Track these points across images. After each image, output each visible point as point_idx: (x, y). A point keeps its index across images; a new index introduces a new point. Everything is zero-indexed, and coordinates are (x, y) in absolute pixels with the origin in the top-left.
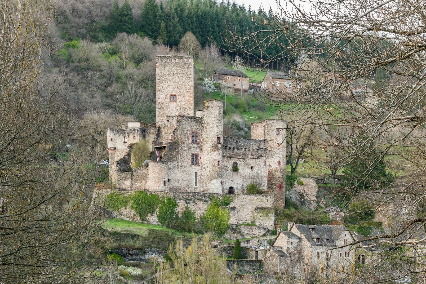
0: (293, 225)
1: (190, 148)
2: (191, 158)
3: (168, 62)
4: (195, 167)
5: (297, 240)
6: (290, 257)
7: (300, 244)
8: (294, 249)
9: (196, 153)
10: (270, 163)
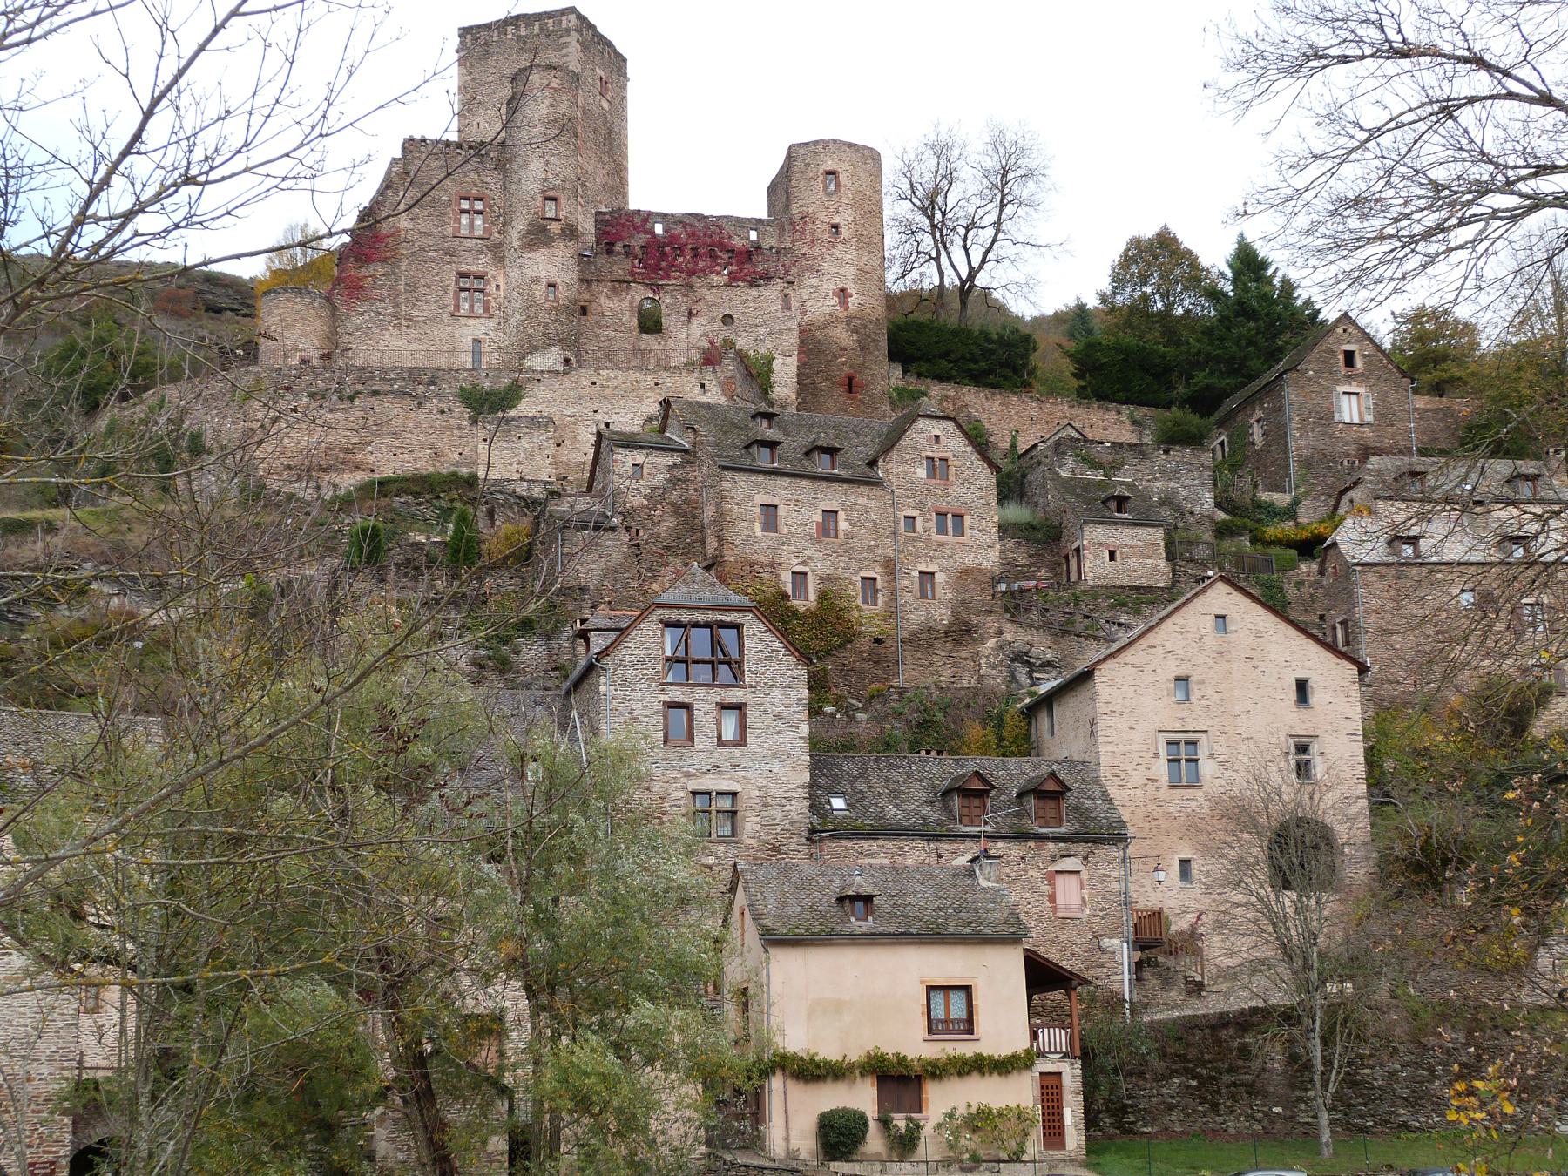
1: (450, 252)
3: (495, 39)
5: (676, 459)
6: (628, 529)
8: (649, 498)
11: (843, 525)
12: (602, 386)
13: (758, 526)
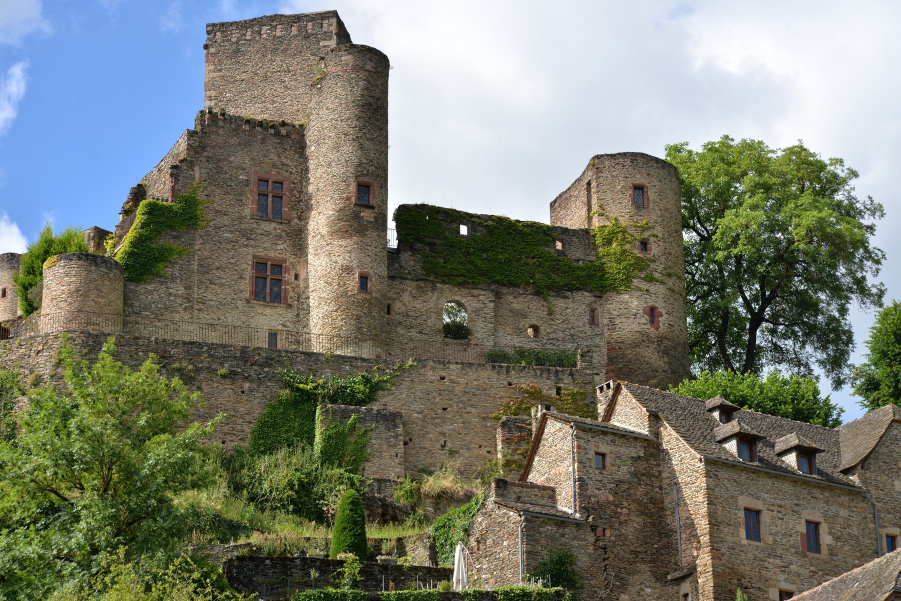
0: (618, 390)
1: (248, 235)
2: (249, 273)
4: (268, 311)
7: (655, 471)
9: (272, 254)
10: (615, 313)
11: (826, 539)
12: (451, 381)
13: (743, 532)
